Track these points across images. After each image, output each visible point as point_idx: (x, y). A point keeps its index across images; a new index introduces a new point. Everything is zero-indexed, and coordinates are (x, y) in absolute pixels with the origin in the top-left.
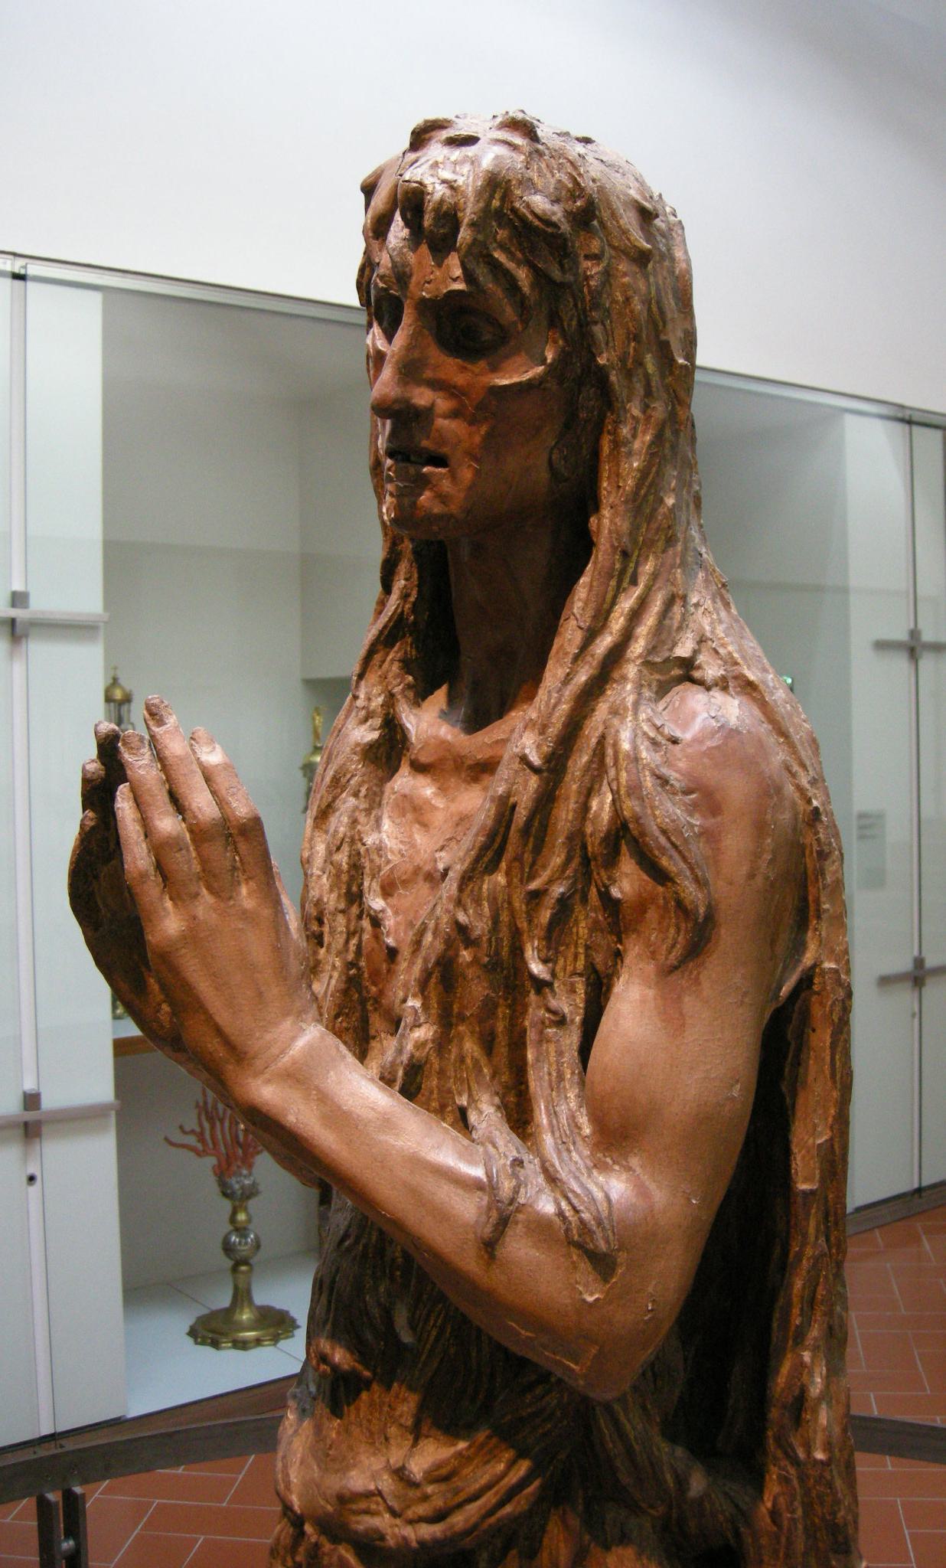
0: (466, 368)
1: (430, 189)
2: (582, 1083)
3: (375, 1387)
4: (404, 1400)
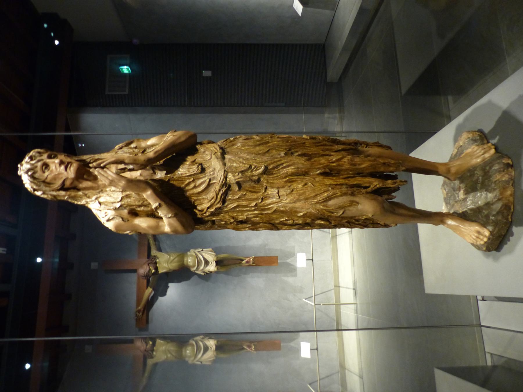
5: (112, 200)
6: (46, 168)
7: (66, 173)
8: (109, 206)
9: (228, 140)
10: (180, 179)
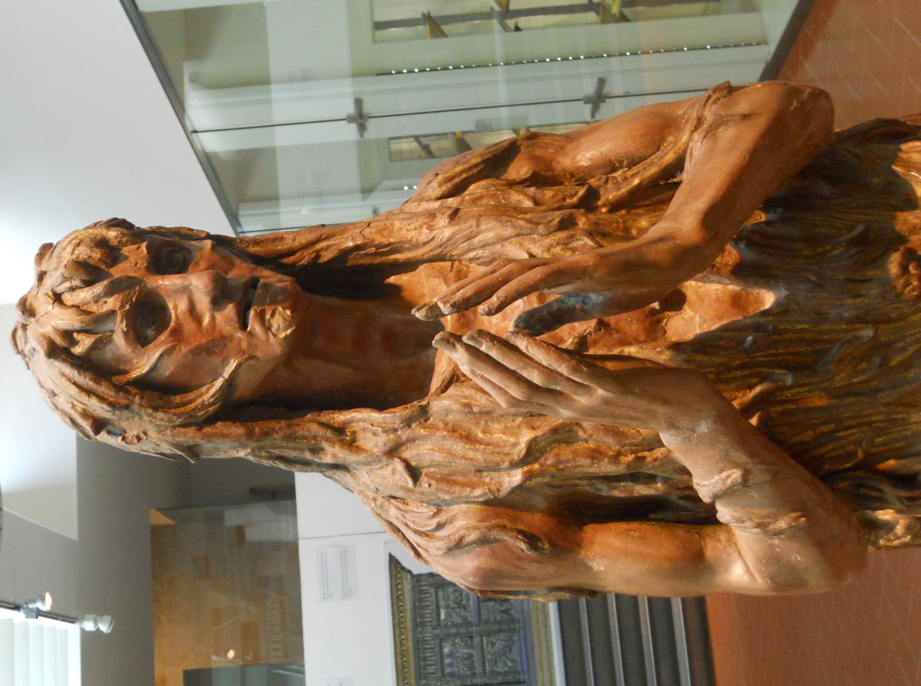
0: (196, 262)
1: (74, 257)
2: (645, 159)
3: (909, 245)
4: (905, 220)
5: (478, 456)
7: (240, 335)
8: (463, 485)
10: (808, 336)
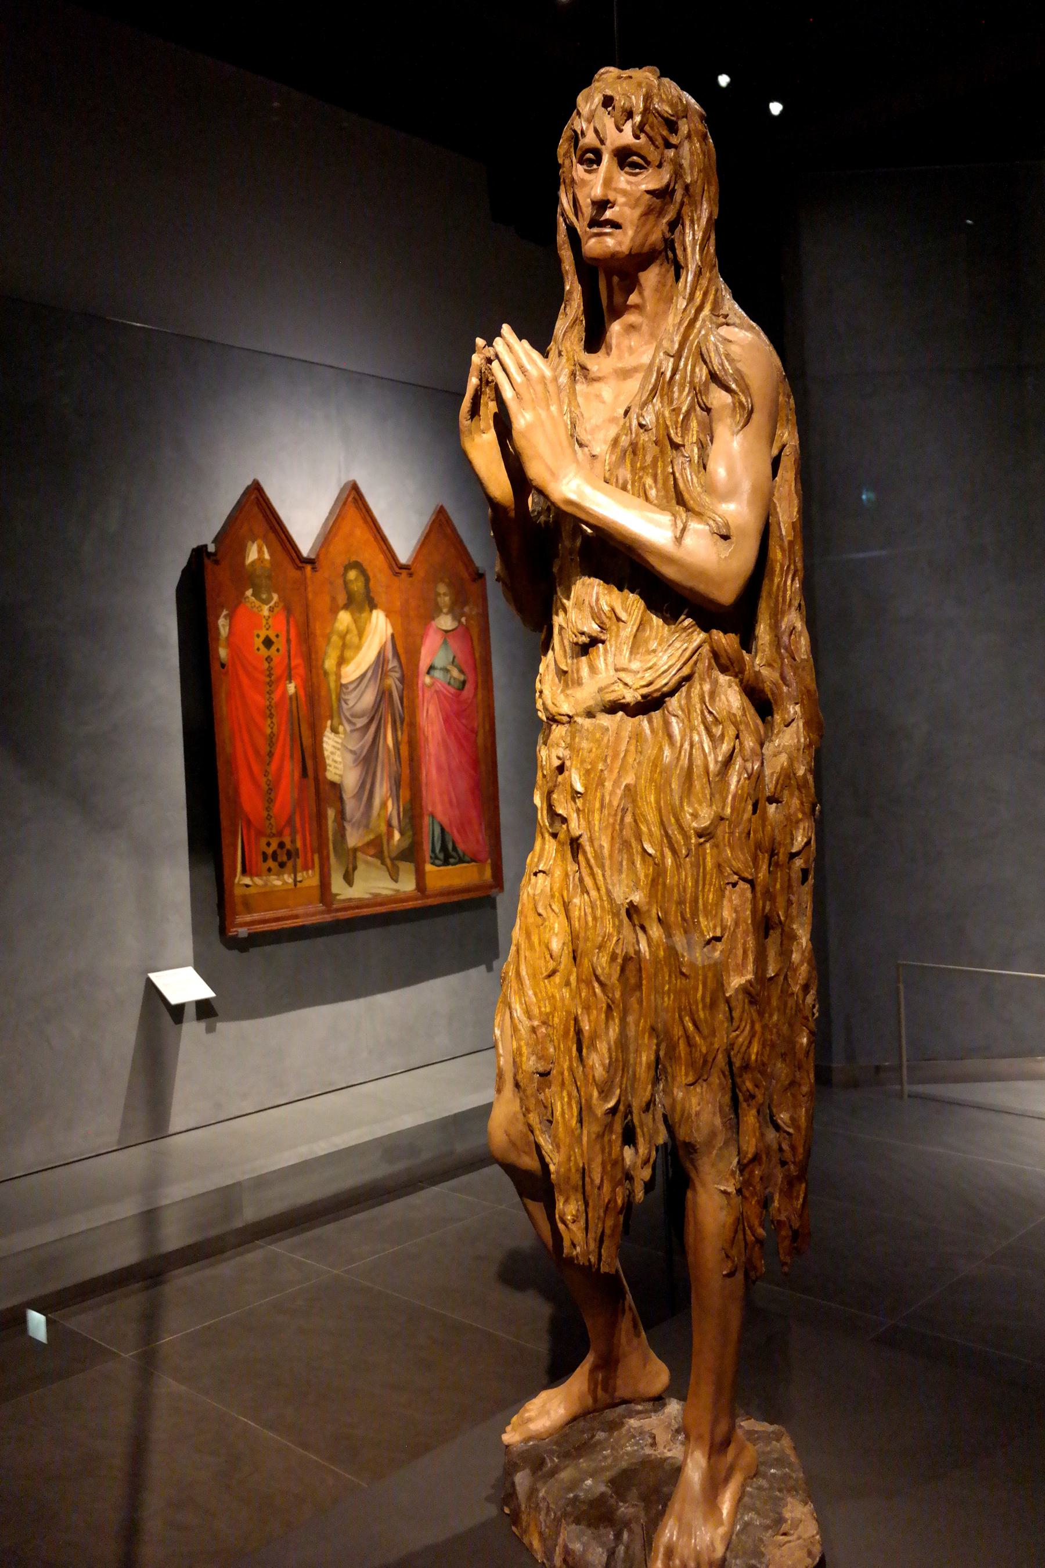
6: (590, 162)
9: (710, 718)
